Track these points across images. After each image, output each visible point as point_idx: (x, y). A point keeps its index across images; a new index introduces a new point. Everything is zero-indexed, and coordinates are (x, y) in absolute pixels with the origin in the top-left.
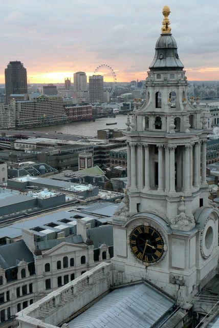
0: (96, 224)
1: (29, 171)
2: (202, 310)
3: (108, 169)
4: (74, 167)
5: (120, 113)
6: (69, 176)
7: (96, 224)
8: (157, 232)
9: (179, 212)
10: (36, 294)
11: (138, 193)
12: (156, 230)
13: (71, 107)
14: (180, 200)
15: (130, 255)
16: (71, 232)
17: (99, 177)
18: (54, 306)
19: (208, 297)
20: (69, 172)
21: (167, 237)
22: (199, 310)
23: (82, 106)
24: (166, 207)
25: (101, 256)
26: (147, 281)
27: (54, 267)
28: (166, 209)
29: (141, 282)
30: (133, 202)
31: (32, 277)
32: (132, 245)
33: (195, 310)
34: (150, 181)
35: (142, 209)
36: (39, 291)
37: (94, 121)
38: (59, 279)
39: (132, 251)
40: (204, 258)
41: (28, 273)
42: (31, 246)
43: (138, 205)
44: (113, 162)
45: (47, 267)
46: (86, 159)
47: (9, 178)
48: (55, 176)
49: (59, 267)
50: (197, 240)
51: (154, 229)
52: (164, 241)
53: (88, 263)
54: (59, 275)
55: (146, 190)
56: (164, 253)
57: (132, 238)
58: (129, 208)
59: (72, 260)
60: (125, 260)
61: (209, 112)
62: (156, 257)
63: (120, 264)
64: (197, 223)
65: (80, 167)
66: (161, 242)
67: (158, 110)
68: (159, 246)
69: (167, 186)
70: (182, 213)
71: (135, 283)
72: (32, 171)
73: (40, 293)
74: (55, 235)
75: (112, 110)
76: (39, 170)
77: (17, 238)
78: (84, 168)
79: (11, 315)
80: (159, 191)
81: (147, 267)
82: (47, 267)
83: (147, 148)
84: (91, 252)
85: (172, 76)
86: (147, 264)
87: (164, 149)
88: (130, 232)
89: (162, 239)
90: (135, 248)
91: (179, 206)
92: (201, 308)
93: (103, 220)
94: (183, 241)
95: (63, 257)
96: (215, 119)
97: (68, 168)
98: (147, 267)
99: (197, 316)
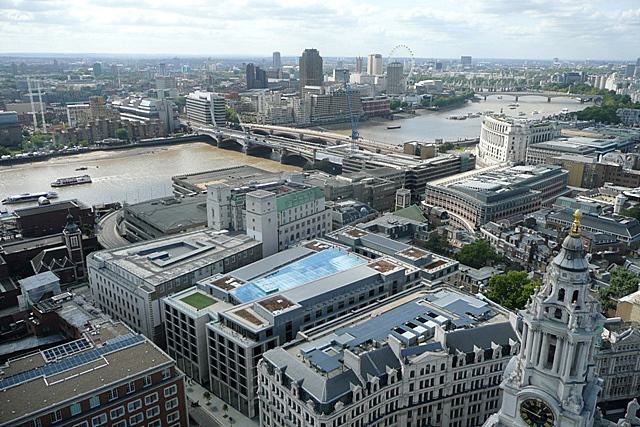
5: (420, 107)
7: (449, 325)
16: (430, 334)
25: (458, 364)
32: (522, 412)
38: (421, 383)
41: (396, 379)
42: (397, 350)
49: (422, 373)
55: (539, 367)
57: (522, 405)
67: (560, 303)
68: (549, 420)
74: (415, 341)
84: (451, 360)
85: (578, 277)
87: (562, 341)
90: (526, 415)
91: (571, 389)
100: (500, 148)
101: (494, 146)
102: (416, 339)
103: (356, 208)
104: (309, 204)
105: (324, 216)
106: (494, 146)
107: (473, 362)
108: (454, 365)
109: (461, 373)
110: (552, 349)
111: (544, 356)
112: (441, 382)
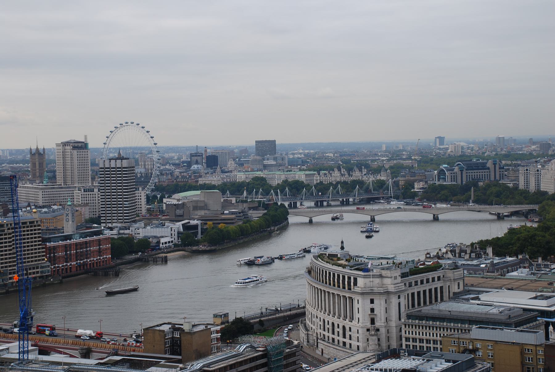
5: (176, 248)
23: (88, 238)
61: (399, 279)
75: (158, 242)
96: (413, 294)
101: (336, 321)
106: (336, 321)
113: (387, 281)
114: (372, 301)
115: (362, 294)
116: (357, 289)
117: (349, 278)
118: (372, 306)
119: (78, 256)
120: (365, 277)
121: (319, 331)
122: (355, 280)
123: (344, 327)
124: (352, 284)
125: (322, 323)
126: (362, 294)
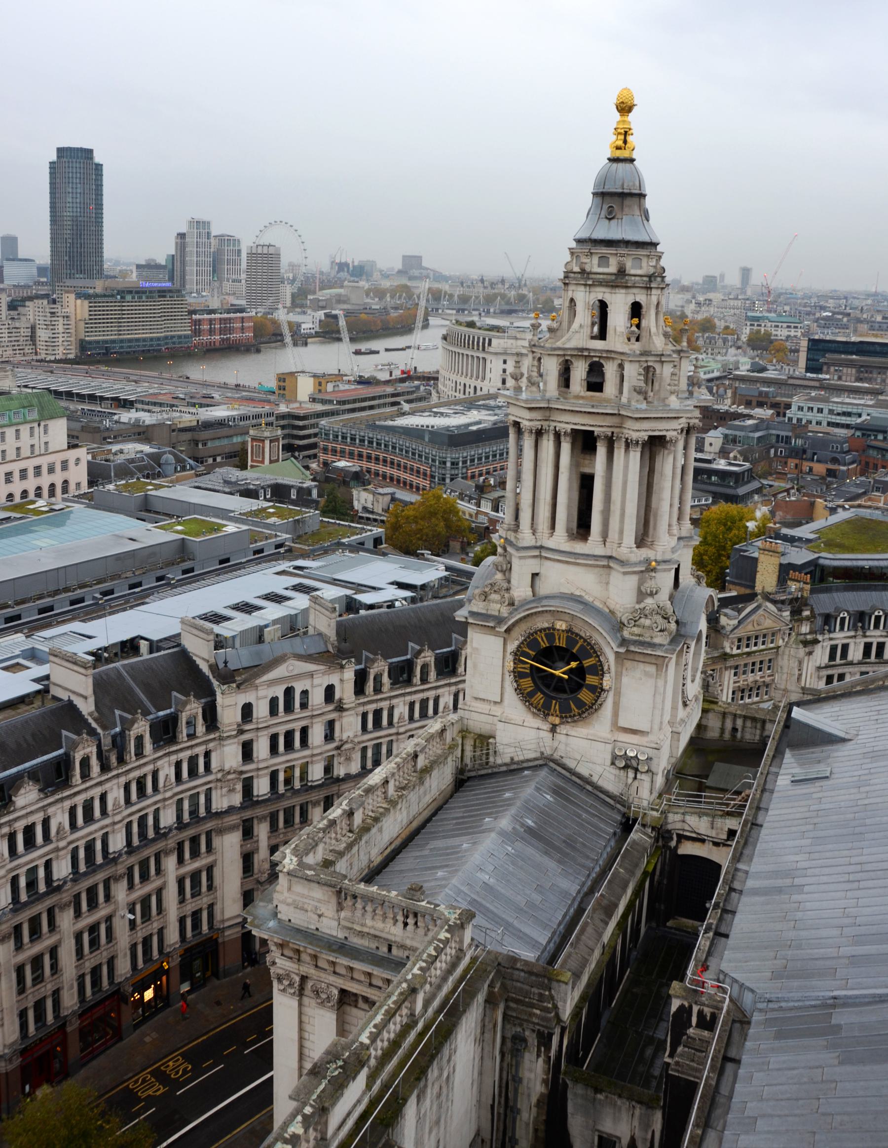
0: (351, 606)
1: (137, 468)
2: (687, 828)
3: (314, 466)
4: (239, 459)
5: (317, 335)
6: (235, 483)
7: (351, 606)
8: (589, 644)
9: (641, 595)
10: (219, 776)
11: (536, 548)
12: (585, 641)
13: (206, 316)
14: (649, 569)
15: (512, 698)
17: (305, 485)
18: (350, 831)
19: (700, 796)
20: (234, 474)
21: (611, 657)
22: (679, 826)
23: (232, 315)
24: (607, 583)
25: (370, 685)
26: (554, 761)
27: (261, 710)
28: (607, 590)
29: (540, 762)
30: (522, 569)
31: (212, 736)
32: (518, 675)
33: (670, 827)
34: (569, 521)
35: (544, 588)
36: (227, 767)
37: (258, 351)
38: (274, 739)
39: (519, 690)
40: (685, 705)
41: (201, 728)
43: (535, 576)
44: (325, 450)
45: (247, 711)
46: (267, 443)
47: (91, 483)
48: (204, 481)
49: (273, 711)
50: (677, 664)
51: (581, 637)
52: (606, 668)
53: (340, 700)
54: (273, 730)
55: (560, 540)
56: (603, 695)
58: (509, 582)
59: (305, 693)
60: (497, 710)
62: (580, 704)
63: (483, 718)
64: (677, 622)
65: (252, 461)
66: (599, 670)
69: (613, 535)
70: (649, 602)
71: (525, 765)
72: (145, 467)
73: (229, 773)
74: (259, 635)
76: (159, 465)
77: (165, 639)
78: (263, 462)
79: (162, 826)
80: (593, 545)
81: (553, 729)
82: (247, 711)
83: (568, 439)
84: (349, 674)
86: (557, 721)
88: (517, 643)
89: (600, 661)
90: (527, 683)
92: (684, 821)
93: (367, 598)
94: (652, 669)
95: (284, 687)
97: (219, 459)
98: (553, 729)
99: (672, 839)
100: (479, 383)
101: (468, 381)
102: (261, 629)
103: (149, 455)
104: (25, 430)
105: (65, 465)
106: (468, 381)
107: (409, 682)
108: (359, 690)
109: (378, 714)
110: (586, 483)
111: (569, 507)
112: (329, 736)
113: (520, 343)
114: (505, 362)
115: (496, 354)
116: (491, 350)
117: (484, 339)
118: (505, 366)
119: (222, 331)
120: (498, 337)
121: (450, 393)
122: (490, 341)
123: (475, 388)
124: (486, 345)
125: (454, 385)
126: (496, 354)
